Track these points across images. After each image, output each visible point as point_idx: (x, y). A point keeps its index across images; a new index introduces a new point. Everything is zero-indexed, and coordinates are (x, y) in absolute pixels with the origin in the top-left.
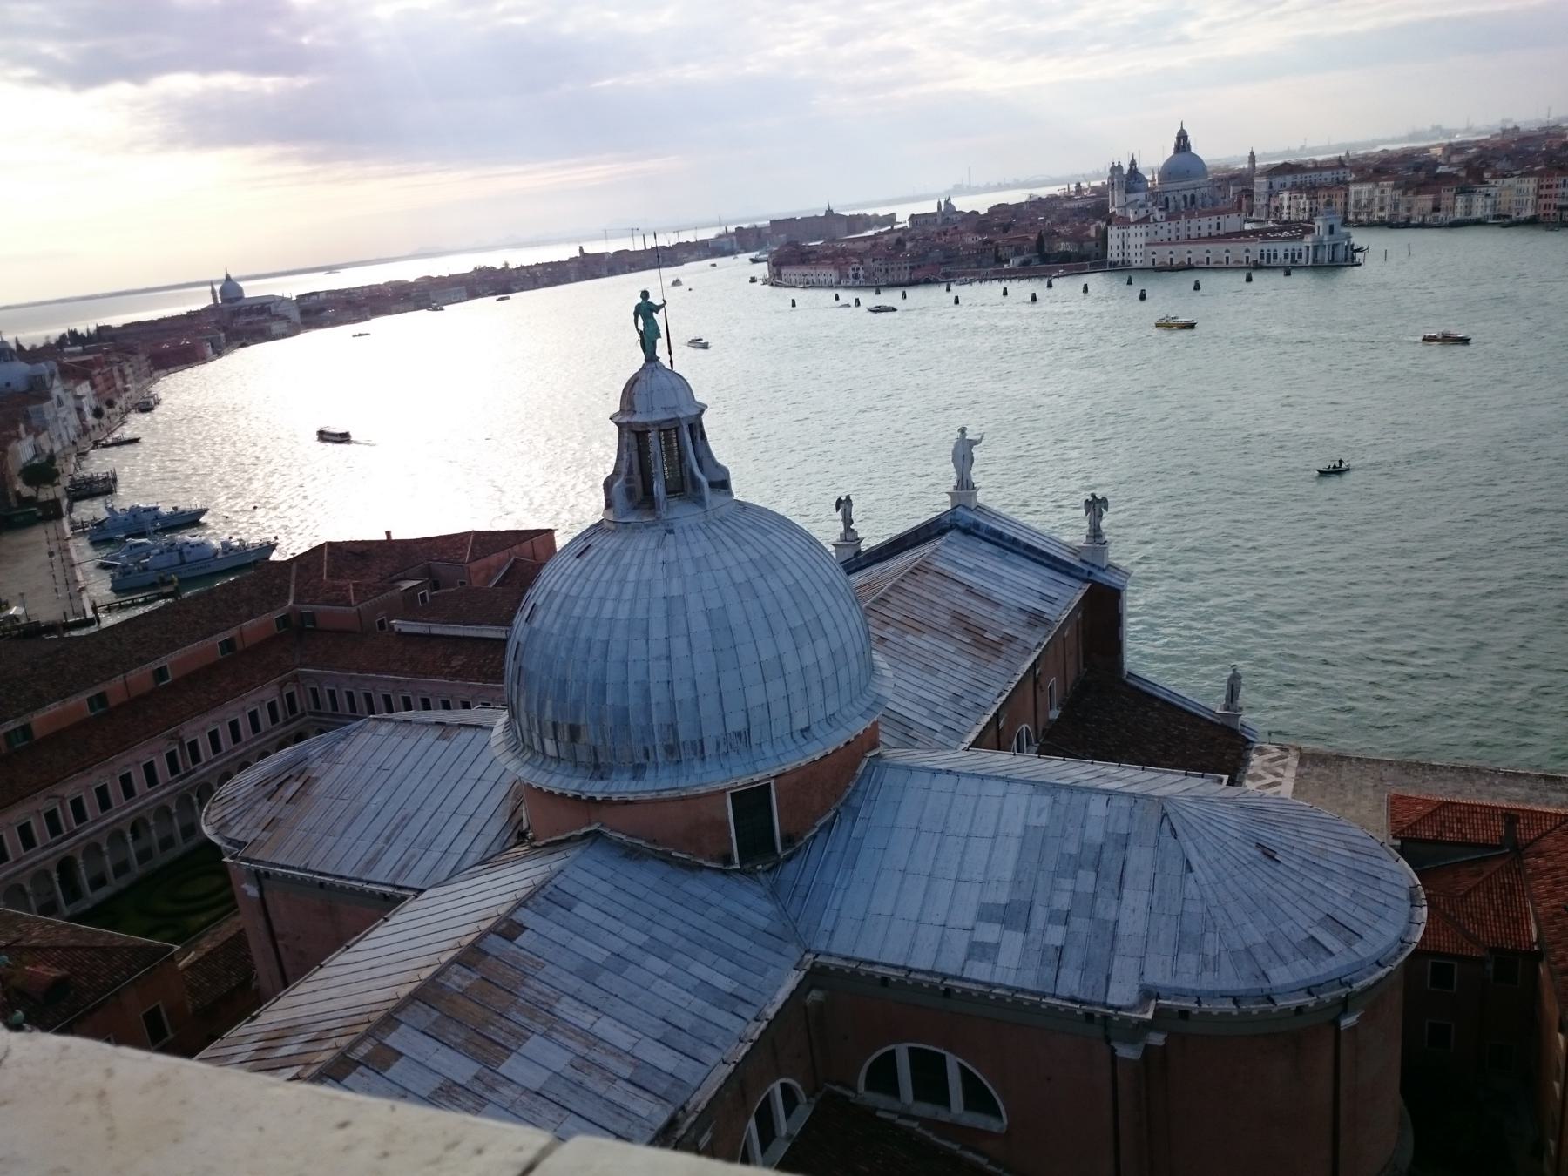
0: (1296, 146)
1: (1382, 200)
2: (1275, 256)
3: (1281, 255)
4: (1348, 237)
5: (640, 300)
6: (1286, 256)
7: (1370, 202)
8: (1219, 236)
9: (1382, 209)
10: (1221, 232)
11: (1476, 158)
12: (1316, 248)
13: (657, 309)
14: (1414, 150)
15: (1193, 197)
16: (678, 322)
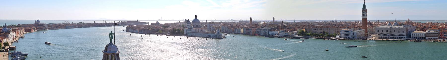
0: (212, 20)
1: (225, 29)
2: (210, 36)
3: (211, 36)
4: (221, 34)
5: (110, 32)
6: (212, 36)
7: (224, 29)
8: (202, 32)
9: (225, 30)
10: (202, 31)
11: (238, 24)
12: (216, 35)
13: (113, 34)
14: (229, 22)
15: (198, 25)
16: (116, 35)
